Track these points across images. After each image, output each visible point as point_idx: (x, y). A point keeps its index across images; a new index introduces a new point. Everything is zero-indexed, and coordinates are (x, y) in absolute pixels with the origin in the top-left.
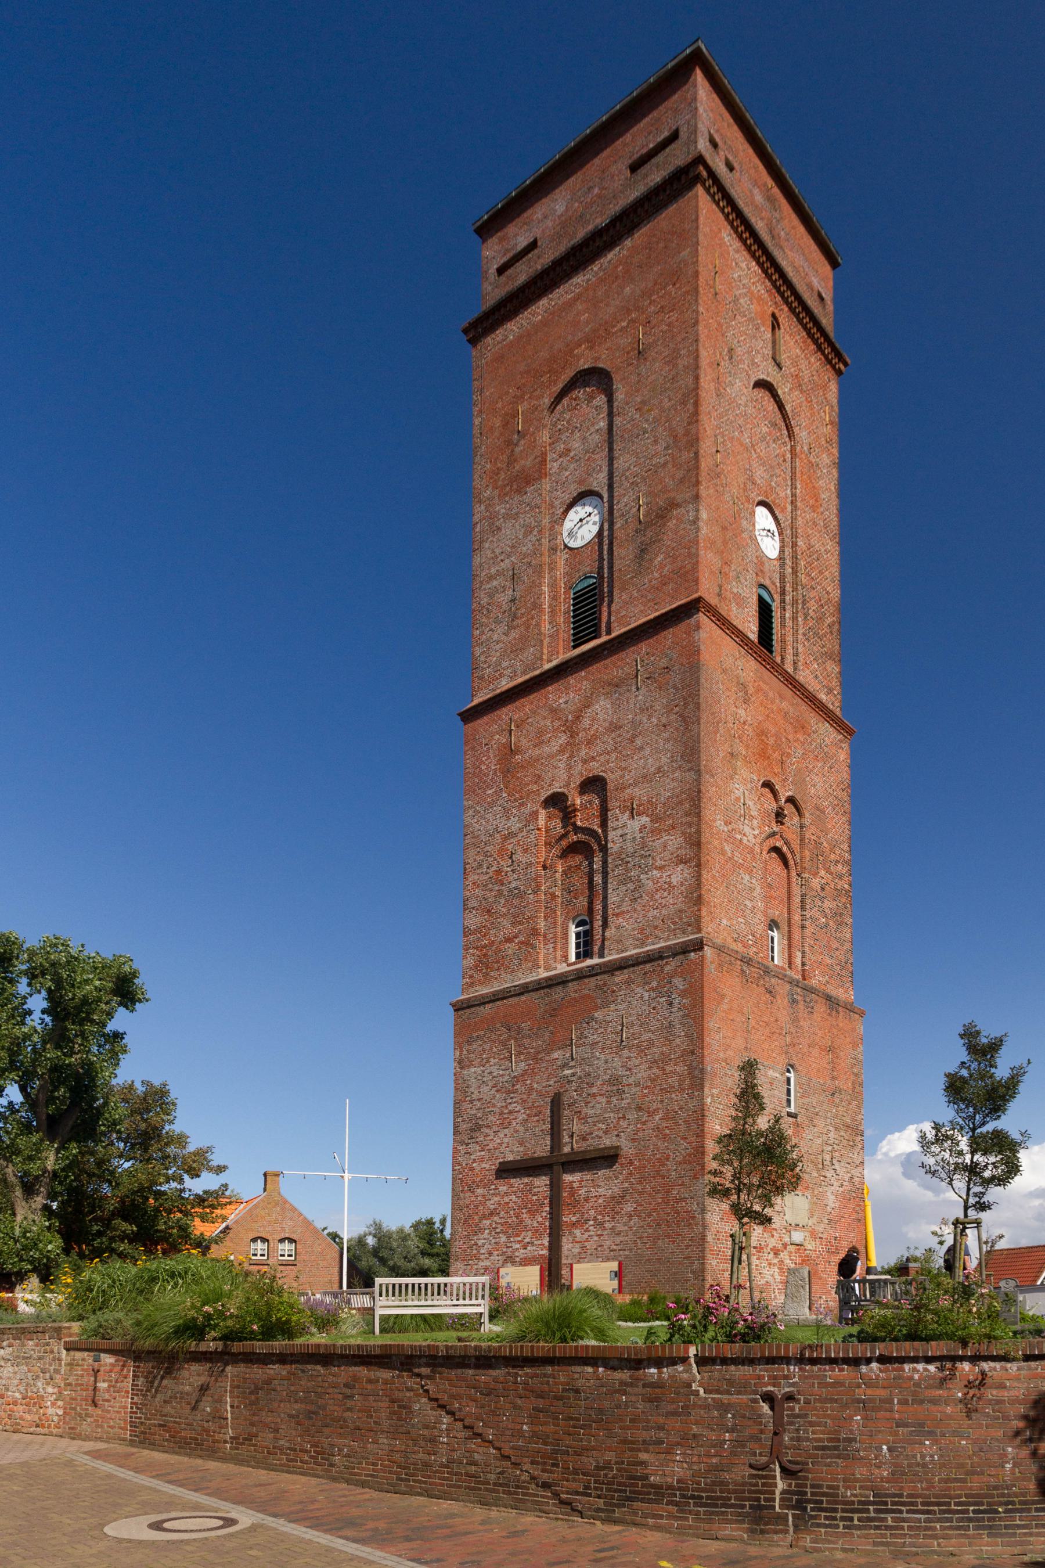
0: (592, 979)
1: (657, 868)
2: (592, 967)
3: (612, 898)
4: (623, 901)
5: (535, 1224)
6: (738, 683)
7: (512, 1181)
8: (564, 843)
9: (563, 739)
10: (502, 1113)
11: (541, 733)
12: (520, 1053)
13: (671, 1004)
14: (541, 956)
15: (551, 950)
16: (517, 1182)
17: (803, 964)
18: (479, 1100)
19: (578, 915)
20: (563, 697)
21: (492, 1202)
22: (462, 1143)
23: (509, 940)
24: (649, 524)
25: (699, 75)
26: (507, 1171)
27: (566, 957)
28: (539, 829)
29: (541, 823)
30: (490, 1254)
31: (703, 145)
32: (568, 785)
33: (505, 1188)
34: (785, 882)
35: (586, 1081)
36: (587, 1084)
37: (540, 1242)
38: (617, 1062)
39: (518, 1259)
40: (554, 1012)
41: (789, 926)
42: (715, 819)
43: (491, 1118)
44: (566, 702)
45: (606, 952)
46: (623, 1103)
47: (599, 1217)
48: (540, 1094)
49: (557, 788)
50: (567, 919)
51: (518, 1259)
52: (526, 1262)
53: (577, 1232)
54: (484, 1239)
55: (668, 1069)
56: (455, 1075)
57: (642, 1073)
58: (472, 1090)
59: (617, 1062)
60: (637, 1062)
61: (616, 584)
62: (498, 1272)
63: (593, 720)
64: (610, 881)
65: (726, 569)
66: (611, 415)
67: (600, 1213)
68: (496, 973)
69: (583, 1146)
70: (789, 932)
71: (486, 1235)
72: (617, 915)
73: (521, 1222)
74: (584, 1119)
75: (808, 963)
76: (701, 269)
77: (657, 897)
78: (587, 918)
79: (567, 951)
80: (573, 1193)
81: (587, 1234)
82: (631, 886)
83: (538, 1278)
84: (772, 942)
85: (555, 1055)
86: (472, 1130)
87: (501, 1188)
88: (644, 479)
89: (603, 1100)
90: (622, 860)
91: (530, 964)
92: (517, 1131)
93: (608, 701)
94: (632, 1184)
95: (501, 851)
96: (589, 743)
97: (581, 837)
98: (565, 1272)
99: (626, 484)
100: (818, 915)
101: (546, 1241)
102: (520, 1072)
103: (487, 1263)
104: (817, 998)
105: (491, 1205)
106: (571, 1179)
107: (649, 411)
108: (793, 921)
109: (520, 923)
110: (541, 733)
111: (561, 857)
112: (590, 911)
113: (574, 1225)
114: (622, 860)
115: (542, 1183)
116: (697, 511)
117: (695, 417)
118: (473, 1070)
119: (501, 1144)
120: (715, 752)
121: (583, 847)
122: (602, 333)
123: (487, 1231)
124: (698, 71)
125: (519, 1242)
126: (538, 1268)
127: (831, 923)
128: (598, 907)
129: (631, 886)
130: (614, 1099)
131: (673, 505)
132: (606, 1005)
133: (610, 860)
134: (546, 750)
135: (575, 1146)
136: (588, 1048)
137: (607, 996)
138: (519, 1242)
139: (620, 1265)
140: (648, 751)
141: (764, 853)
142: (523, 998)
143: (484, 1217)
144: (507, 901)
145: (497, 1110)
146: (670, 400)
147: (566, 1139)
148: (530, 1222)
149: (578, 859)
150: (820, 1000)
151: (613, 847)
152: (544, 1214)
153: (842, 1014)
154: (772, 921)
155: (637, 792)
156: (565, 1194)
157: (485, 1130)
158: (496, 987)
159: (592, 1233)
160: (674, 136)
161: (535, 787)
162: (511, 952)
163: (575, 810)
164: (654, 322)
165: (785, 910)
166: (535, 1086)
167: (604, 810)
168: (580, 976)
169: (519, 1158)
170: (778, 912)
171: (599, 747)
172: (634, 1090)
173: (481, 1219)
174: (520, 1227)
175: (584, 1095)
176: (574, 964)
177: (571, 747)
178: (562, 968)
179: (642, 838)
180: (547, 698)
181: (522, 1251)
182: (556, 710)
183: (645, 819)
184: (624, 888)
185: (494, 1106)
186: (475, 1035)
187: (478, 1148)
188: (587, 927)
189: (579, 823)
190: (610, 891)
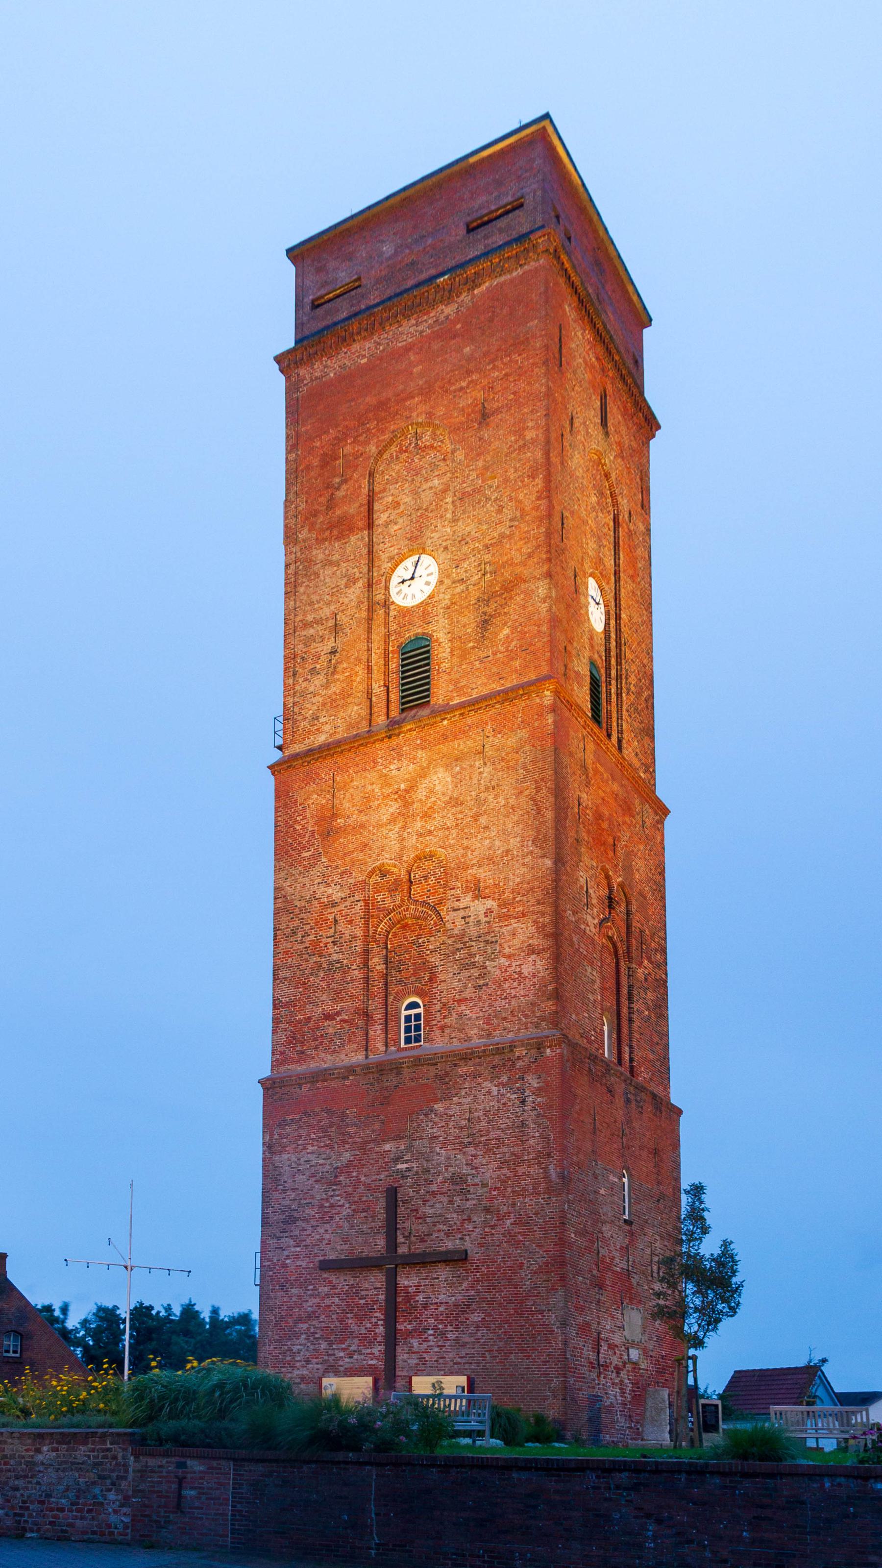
0: (432, 1068)
5: (363, 1331)
10: (321, 1206)
11: (368, 798)
12: (344, 1142)
13: (523, 1102)
16: (343, 1281)
21: (310, 1304)
27: (397, 1042)
30: (308, 1361)
33: (326, 1289)
36: (426, 1180)
37: (369, 1351)
39: (342, 1369)
43: (309, 1211)
46: (469, 1204)
47: (440, 1326)
48: (368, 1188)
51: (342, 1369)
53: (415, 1342)
55: (521, 1170)
60: (484, 1162)
69: (419, 1248)
73: (347, 1327)
80: (408, 1298)
81: (425, 1345)
85: (387, 1147)
87: (320, 1289)
94: (478, 1292)
106: (406, 1283)
110: (368, 798)
113: (410, 1334)
119: (321, 1240)
123: (303, 1336)
125: (344, 1350)
136: (426, 1142)
138: (344, 1350)
142: (347, 1082)
143: (300, 1320)
147: (400, 1239)
156: (399, 1299)
159: (431, 1343)
161: (361, 856)
166: (363, 1179)
169: (343, 1257)
173: (296, 1322)
174: (344, 1334)
177: (404, 816)
180: (375, 762)
181: (348, 1360)
182: (386, 775)
184: (466, 974)
185: (312, 1197)
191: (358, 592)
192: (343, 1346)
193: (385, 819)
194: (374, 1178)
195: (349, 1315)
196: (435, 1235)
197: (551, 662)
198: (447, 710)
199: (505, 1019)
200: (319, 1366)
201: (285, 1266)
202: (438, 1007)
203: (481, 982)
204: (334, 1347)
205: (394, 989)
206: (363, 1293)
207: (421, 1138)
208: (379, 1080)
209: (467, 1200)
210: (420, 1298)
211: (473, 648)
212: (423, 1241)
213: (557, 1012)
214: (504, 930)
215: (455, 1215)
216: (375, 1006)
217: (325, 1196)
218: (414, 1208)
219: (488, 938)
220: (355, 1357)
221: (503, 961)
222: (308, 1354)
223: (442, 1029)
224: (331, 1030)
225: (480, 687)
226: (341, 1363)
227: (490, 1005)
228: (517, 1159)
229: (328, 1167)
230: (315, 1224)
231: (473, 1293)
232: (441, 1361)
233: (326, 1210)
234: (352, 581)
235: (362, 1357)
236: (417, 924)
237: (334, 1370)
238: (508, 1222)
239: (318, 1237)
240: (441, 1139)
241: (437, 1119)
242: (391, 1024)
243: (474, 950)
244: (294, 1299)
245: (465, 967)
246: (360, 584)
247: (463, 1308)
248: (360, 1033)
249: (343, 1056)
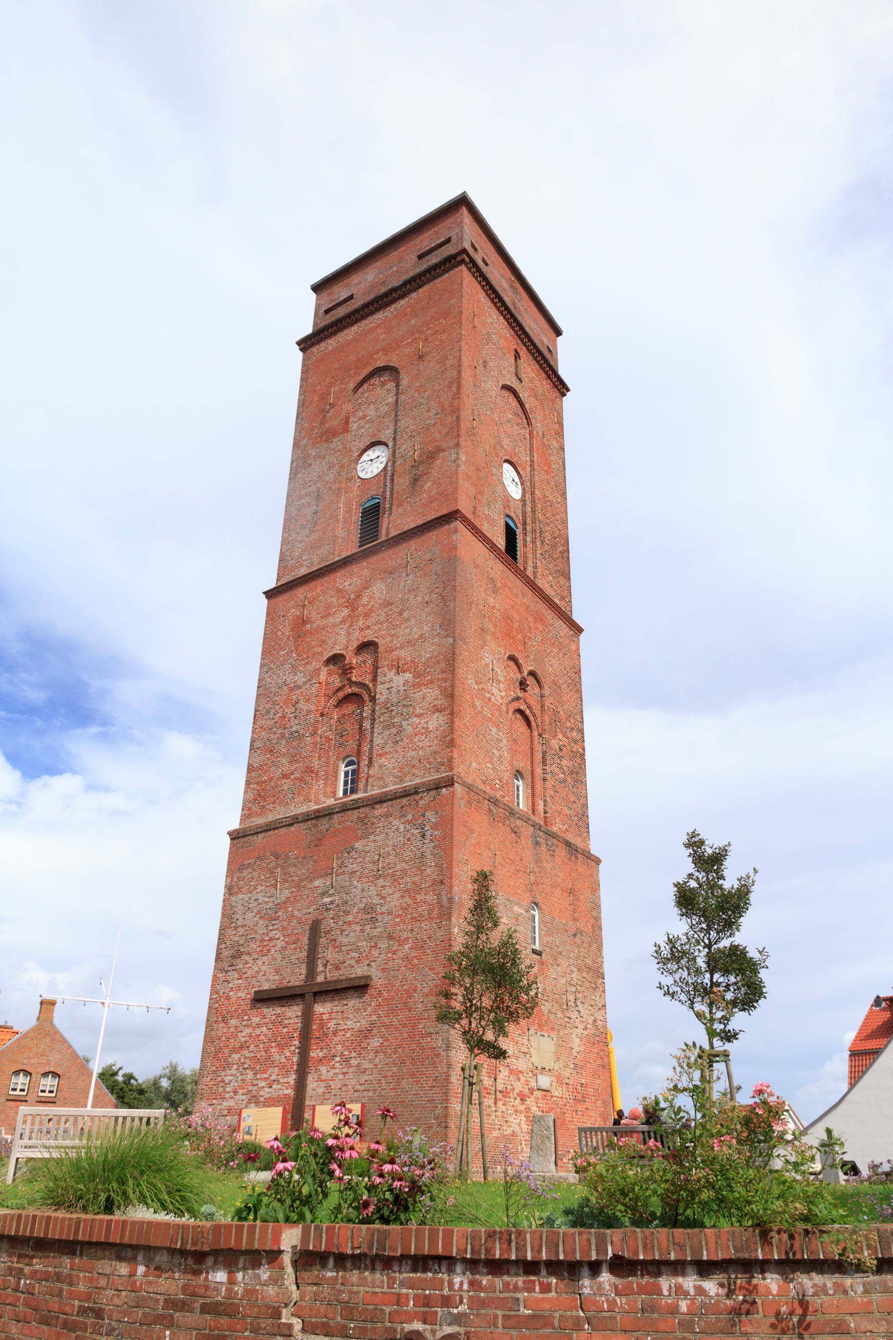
0: (355, 812)
1: (416, 716)
2: (356, 800)
3: (378, 741)
4: (386, 743)
5: (283, 1060)
6: (488, 577)
7: (266, 1011)
8: (340, 695)
9: (345, 612)
10: (262, 940)
12: (285, 881)
14: (313, 792)
15: (322, 786)
16: (271, 1012)
18: (243, 926)
19: (348, 756)
20: (347, 581)
21: (243, 1034)
22: (222, 970)
23: (285, 776)
24: (421, 462)
25: (464, 211)
26: (262, 999)
28: (320, 683)
29: (323, 677)
30: (235, 1092)
31: (467, 245)
32: (347, 648)
34: (528, 741)
35: (343, 909)
36: (344, 912)
37: (285, 1080)
38: (373, 890)
39: (262, 1099)
40: (318, 843)
41: (533, 777)
42: (468, 680)
44: (350, 585)
45: (369, 788)
47: (346, 1053)
49: (337, 650)
50: (338, 759)
51: (262, 1099)
52: (270, 1102)
53: (323, 1069)
54: (231, 1076)
55: (419, 898)
56: (224, 901)
57: (394, 901)
58: (237, 916)
59: (373, 890)
60: (391, 891)
61: (395, 502)
62: (240, 1115)
63: (371, 598)
64: (376, 726)
65: (480, 497)
66: (397, 394)
67: (347, 1048)
68: (272, 806)
70: (533, 782)
71: (233, 1071)
72: (381, 755)
74: (339, 948)
75: (549, 811)
76: (464, 311)
77: (415, 740)
78: (355, 759)
79: (335, 788)
80: (322, 1026)
81: (332, 1072)
82: (394, 731)
83: (280, 1121)
84: (518, 790)
86: (233, 957)
88: (419, 433)
89: (358, 928)
90: (387, 708)
91: (302, 798)
92: (274, 959)
93: (383, 584)
94: (379, 1017)
95: (287, 700)
96: (366, 615)
97: (355, 689)
98: (307, 1116)
99: (406, 437)
101: (292, 1079)
102: (284, 899)
103: (231, 1103)
104: (558, 843)
105: (242, 1037)
106: (322, 1010)
107: (425, 391)
108: (535, 774)
109: (296, 761)
111: (336, 707)
112: (359, 753)
114: (387, 708)
115: (293, 1013)
116: (458, 454)
117: (458, 395)
118: (240, 896)
120: (469, 626)
121: (354, 698)
122: (394, 345)
123: (235, 1067)
124: (464, 208)
126: (280, 1109)
128: (365, 748)
129: (394, 731)
130: (367, 927)
131: (439, 450)
132: (365, 836)
133: (377, 708)
134: (331, 620)
135: (328, 975)
137: (366, 828)
138: (266, 1079)
139: (363, 1107)
140: (413, 622)
141: (510, 713)
142: (292, 829)
143: (234, 1050)
144: (287, 742)
145: (258, 937)
146: (440, 385)
147: (320, 968)
148: (278, 1057)
149: (350, 708)
150: (560, 845)
151: (381, 698)
152: (293, 1048)
153: (580, 860)
154: (518, 771)
155: (402, 653)
157: (245, 957)
158: (270, 817)
159: (337, 1071)
160: (448, 241)
162: (286, 787)
163: (352, 668)
164: (430, 339)
165: (529, 763)
166: (296, 913)
167: (376, 667)
168: (345, 809)
169: (274, 987)
170: (522, 764)
171: (374, 618)
172: (386, 919)
173: (231, 1053)
175: (341, 923)
176: (341, 798)
177: (351, 618)
178: (331, 802)
179: (405, 690)
181: (267, 1090)
183: (408, 676)
186: (246, 863)
187: (237, 976)
188: (355, 767)
189: (354, 679)
190: (376, 735)
192: (266, 1076)
193: (338, 620)
194: (304, 912)
195: (273, 1044)
196: (348, 962)
200: (244, 1097)
204: (258, 1076)
206: (286, 1022)
207: (344, 873)
208: (315, 826)
209: (375, 928)
210: (332, 1024)
212: (337, 968)
215: (365, 943)
217: (265, 931)
218: (333, 938)
220: (274, 1086)
222: (236, 1084)
226: (262, 1093)
228: (417, 888)
230: (256, 957)
231: (374, 1018)
232: (344, 1089)
233: (265, 943)
235: (280, 1086)
237: (254, 1100)
238: (407, 947)
239: (256, 969)
240: (358, 873)
244: (232, 1030)
247: (366, 1033)
249: (292, 808)
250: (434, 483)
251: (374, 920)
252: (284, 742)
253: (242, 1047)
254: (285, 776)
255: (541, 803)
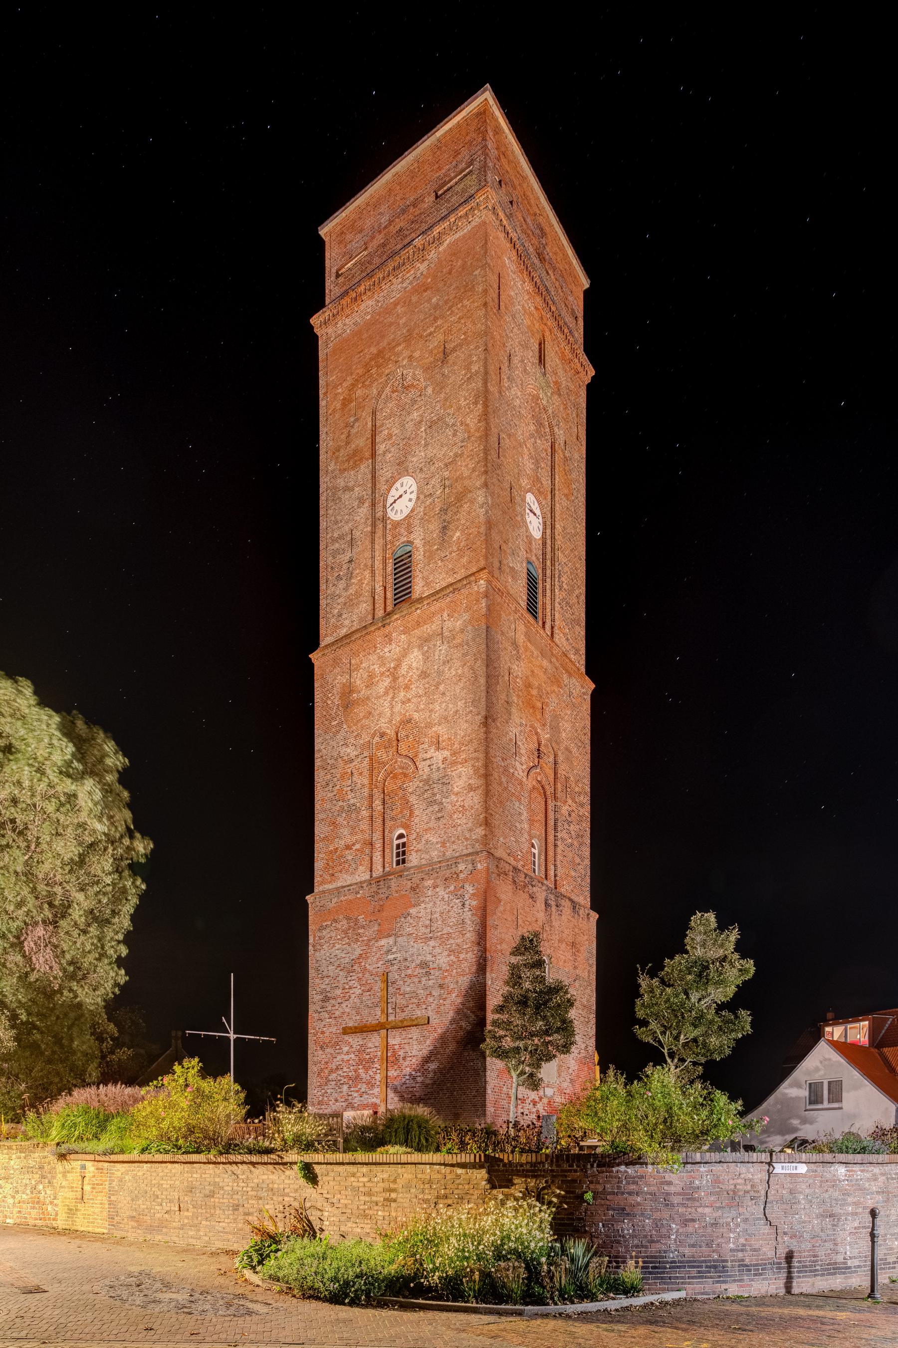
12: (357, 940)
17: (555, 876)
23: (348, 847)
86: (323, 1001)
100: (566, 836)
125: (357, 1091)
127: (575, 843)
142: (358, 896)
162: (350, 858)
184: (431, 809)
187: (327, 1016)
191: (365, 510)
197: (486, 558)
198: (420, 600)
199: (453, 842)
201: (323, 1033)
202: (414, 836)
203: (439, 815)
205: (389, 824)
211: (438, 549)
213: (486, 835)
214: (453, 774)
216: (377, 836)
219: (444, 780)
221: (453, 798)
223: (417, 851)
224: (350, 858)
225: (441, 580)
227: (445, 833)
229: (347, 960)
234: (361, 501)
236: (402, 773)
241: (411, 921)
242: (387, 851)
243: (436, 790)
245: (431, 803)
246: (366, 505)
248: (368, 858)
250: (463, 531)
251: (428, 974)
252: (344, 815)
253: (337, 1069)
254: (348, 847)
255: (552, 867)
